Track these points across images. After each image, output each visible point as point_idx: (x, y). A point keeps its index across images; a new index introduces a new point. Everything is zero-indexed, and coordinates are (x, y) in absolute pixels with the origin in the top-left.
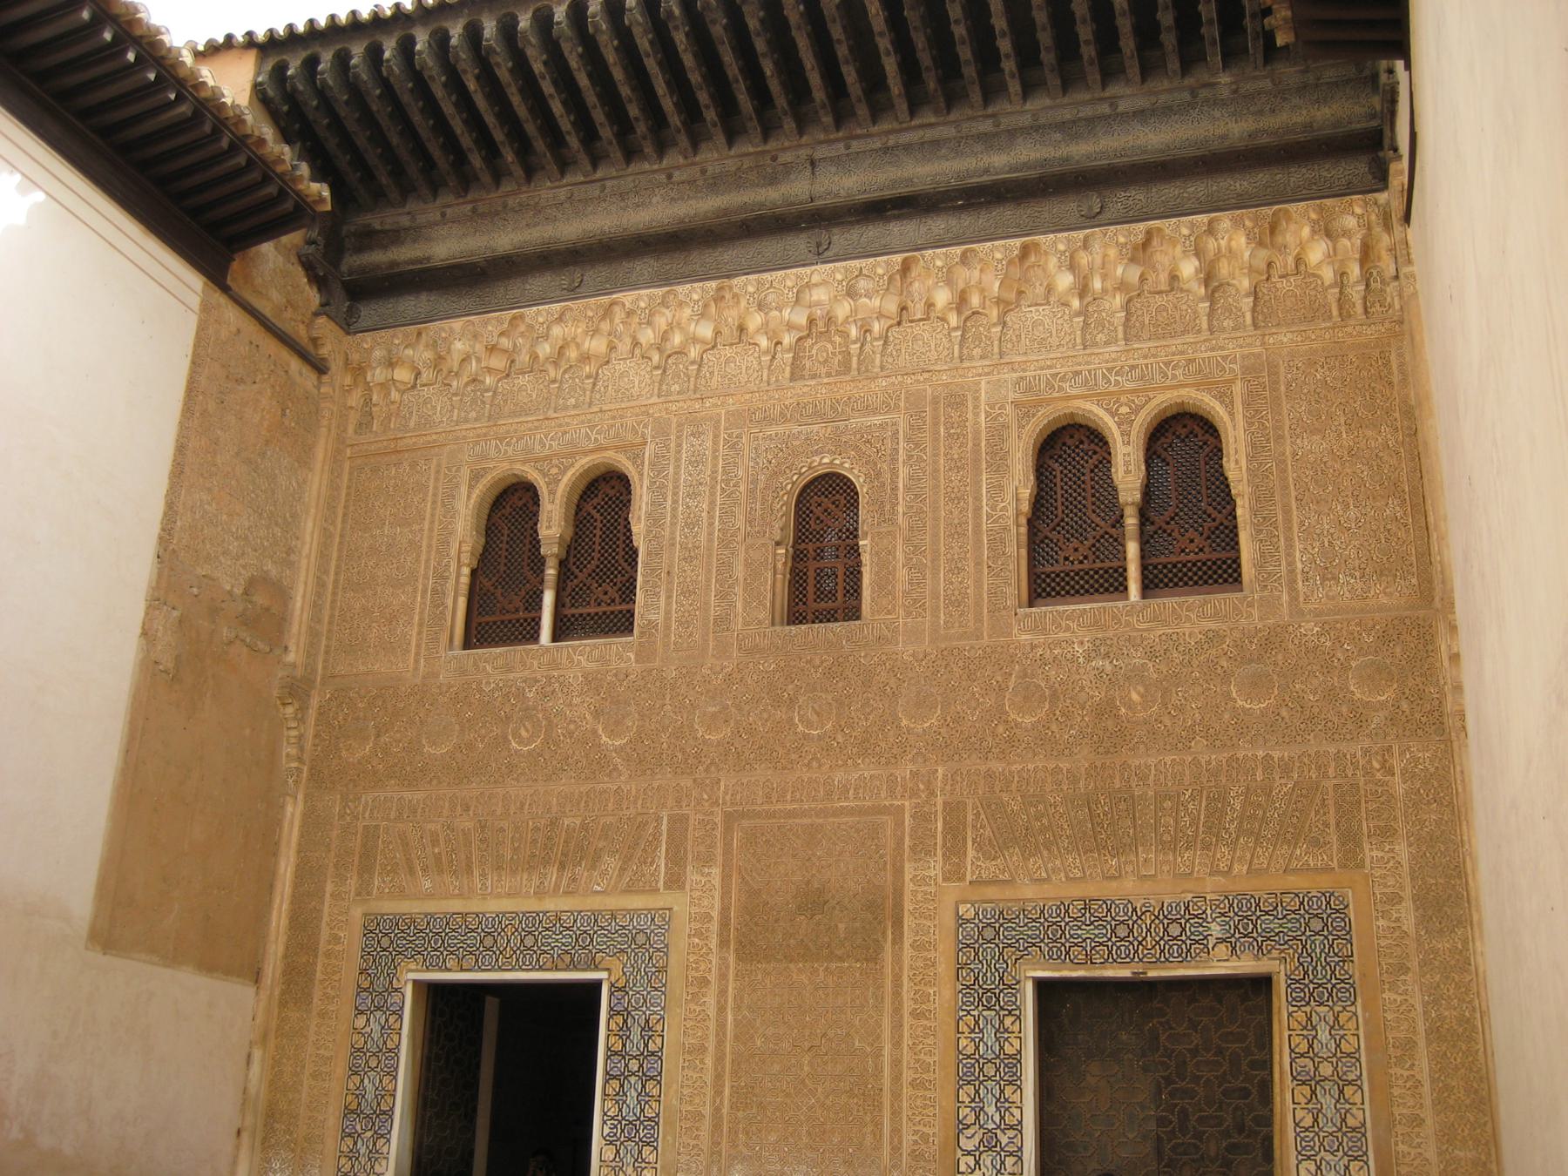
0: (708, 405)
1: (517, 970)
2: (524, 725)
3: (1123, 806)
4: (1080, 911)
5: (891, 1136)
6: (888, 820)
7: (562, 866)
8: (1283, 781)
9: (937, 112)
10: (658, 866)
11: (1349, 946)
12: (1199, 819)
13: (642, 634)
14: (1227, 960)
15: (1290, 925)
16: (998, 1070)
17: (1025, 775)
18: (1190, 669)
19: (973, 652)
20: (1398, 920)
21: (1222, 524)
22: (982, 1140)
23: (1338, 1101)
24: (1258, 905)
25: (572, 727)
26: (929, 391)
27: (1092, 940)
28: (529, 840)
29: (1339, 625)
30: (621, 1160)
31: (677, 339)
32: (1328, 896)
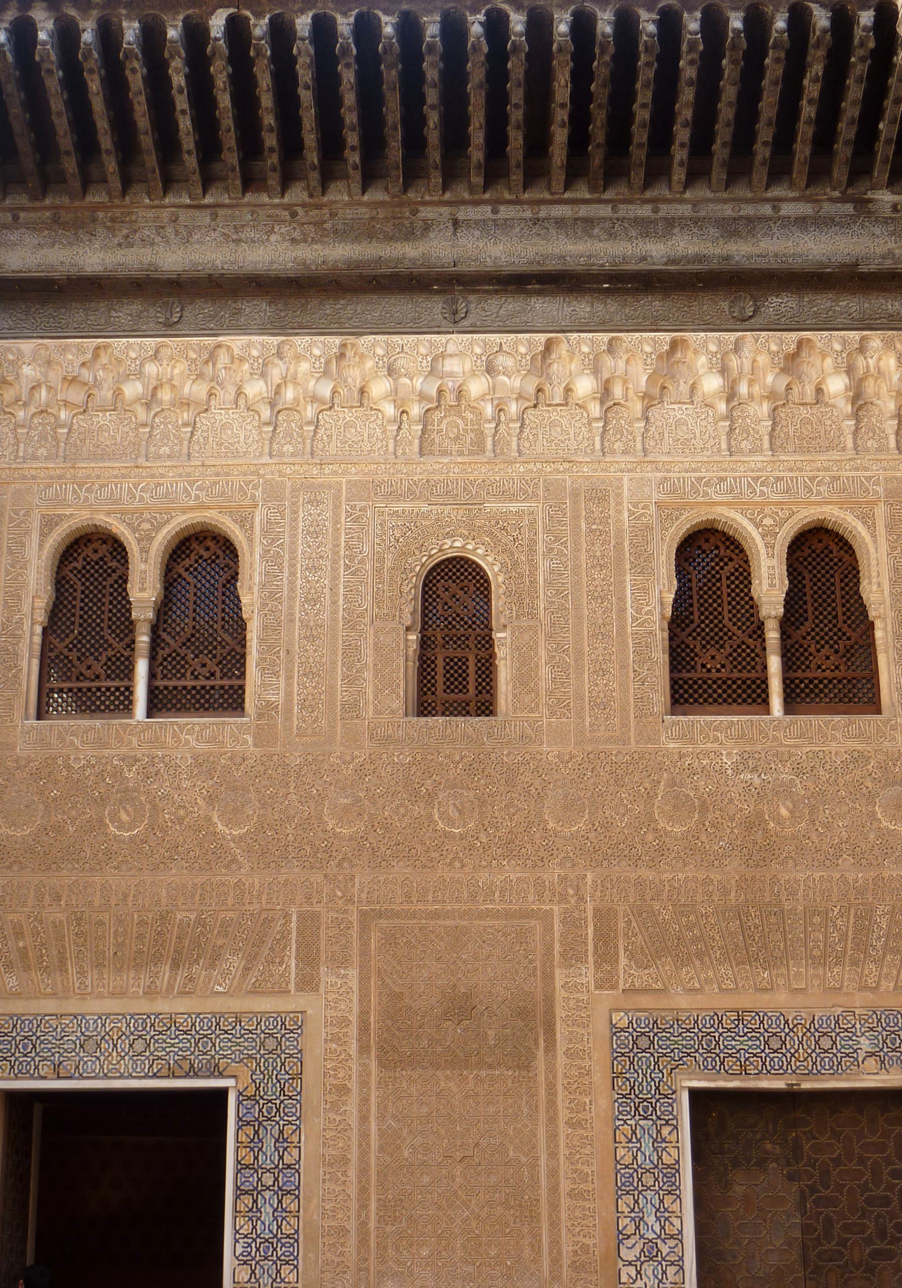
0: (327, 471)
1: (127, 1078)
2: (124, 808)
4: (733, 1022)
5: (550, 1248)
7: (175, 965)
9: (593, 189)
10: (288, 966)
13: (260, 716)
14: (877, 1073)
16: (656, 1180)
18: (837, 788)
19: (620, 757)
21: (856, 643)
22: (642, 1250)
25: (182, 813)
26: (569, 483)
27: (746, 1051)
28: (135, 935)
30: (258, 1281)
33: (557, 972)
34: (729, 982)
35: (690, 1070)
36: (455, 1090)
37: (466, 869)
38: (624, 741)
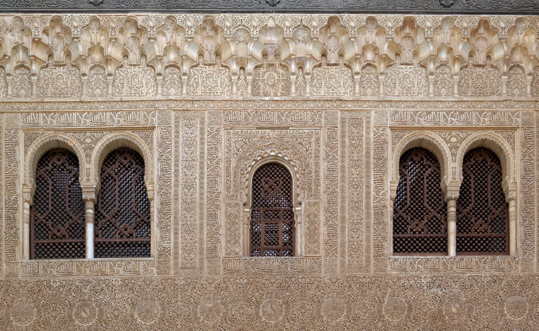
0: (196, 106)
2: (84, 311)
13: (160, 255)
25: (116, 313)
31: (172, 56)
38: (367, 270)
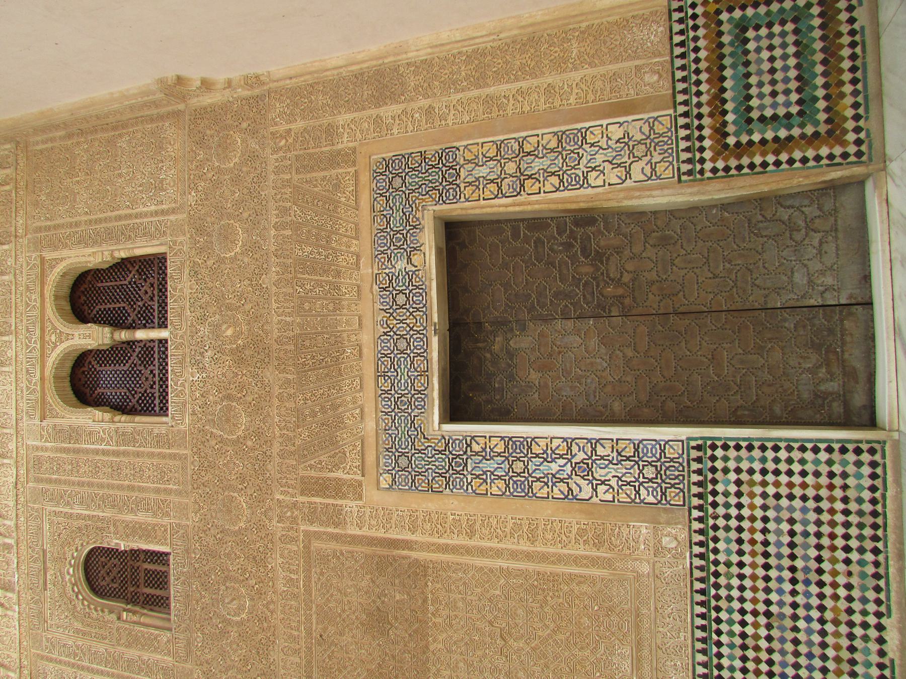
3: (307, 343)
4: (386, 381)
6: (316, 544)
8: (293, 214)
11: (413, 155)
12: (318, 280)
14: (424, 254)
15: (398, 204)
16: (518, 459)
17: (283, 424)
20: (393, 118)
22: (582, 477)
23: (537, 156)
24: (382, 231)
29: (192, 177)
32: (376, 175)
33: (349, 532)
34: (355, 383)
35: (425, 422)
36: (444, 635)
37: (275, 599)
38: (185, 458)
